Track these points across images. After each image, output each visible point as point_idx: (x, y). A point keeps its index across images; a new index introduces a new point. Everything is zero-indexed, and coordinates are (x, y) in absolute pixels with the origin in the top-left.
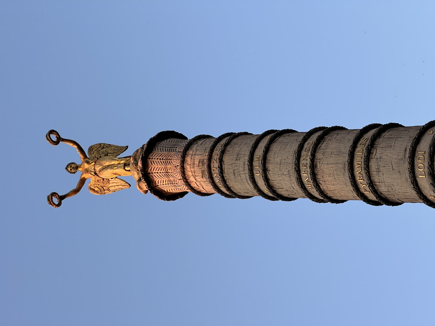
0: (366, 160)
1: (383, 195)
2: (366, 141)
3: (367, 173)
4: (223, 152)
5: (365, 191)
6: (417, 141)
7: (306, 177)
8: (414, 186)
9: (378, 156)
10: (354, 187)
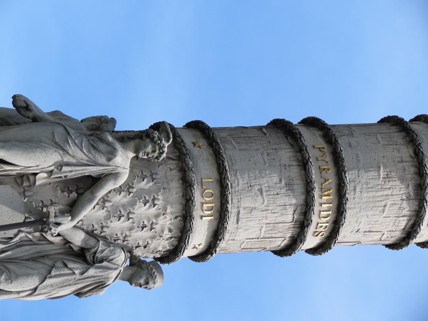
0: (311, 204)
1: (290, 143)
2: (317, 232)
3: (309, 181)
5: (322, 148)
8: (223, 164)
9: (290, 211)
10: (339, 157)
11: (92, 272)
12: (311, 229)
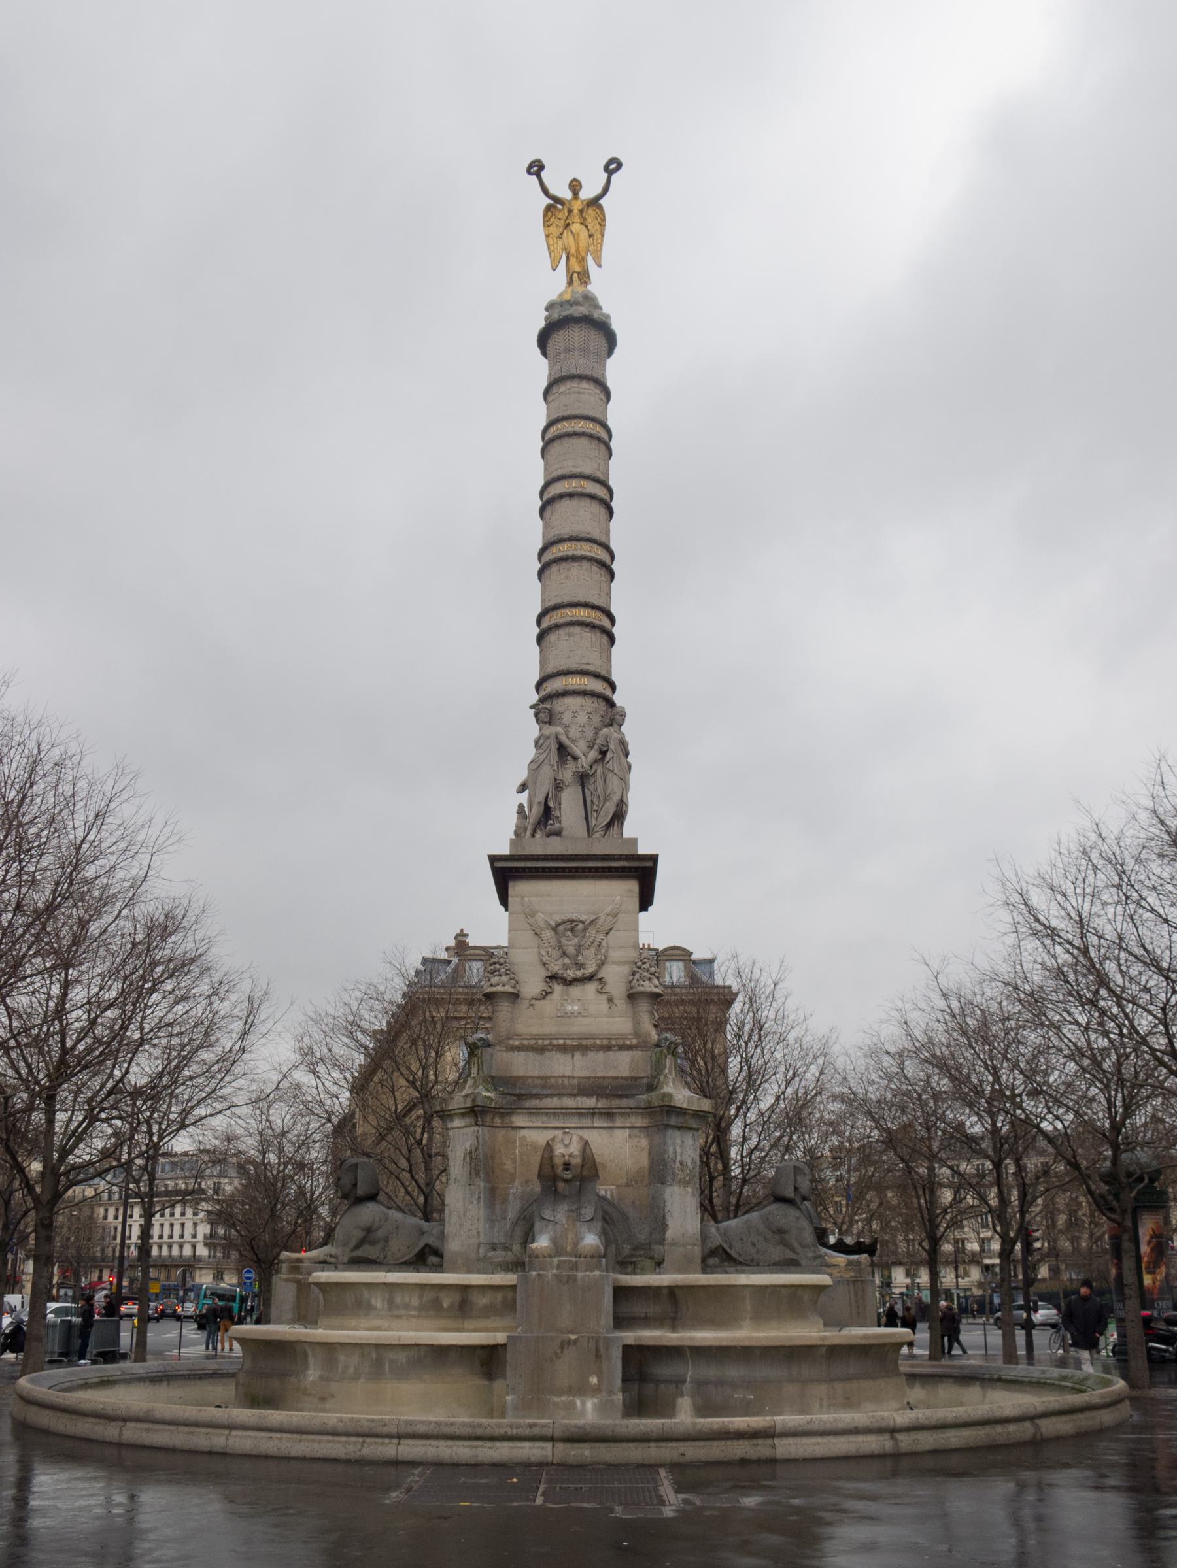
4: (591, 436)
6: (597, 676)
7: (565, 549)
9: (585, 634)
11: (612, 746)
12: (597, 622)
